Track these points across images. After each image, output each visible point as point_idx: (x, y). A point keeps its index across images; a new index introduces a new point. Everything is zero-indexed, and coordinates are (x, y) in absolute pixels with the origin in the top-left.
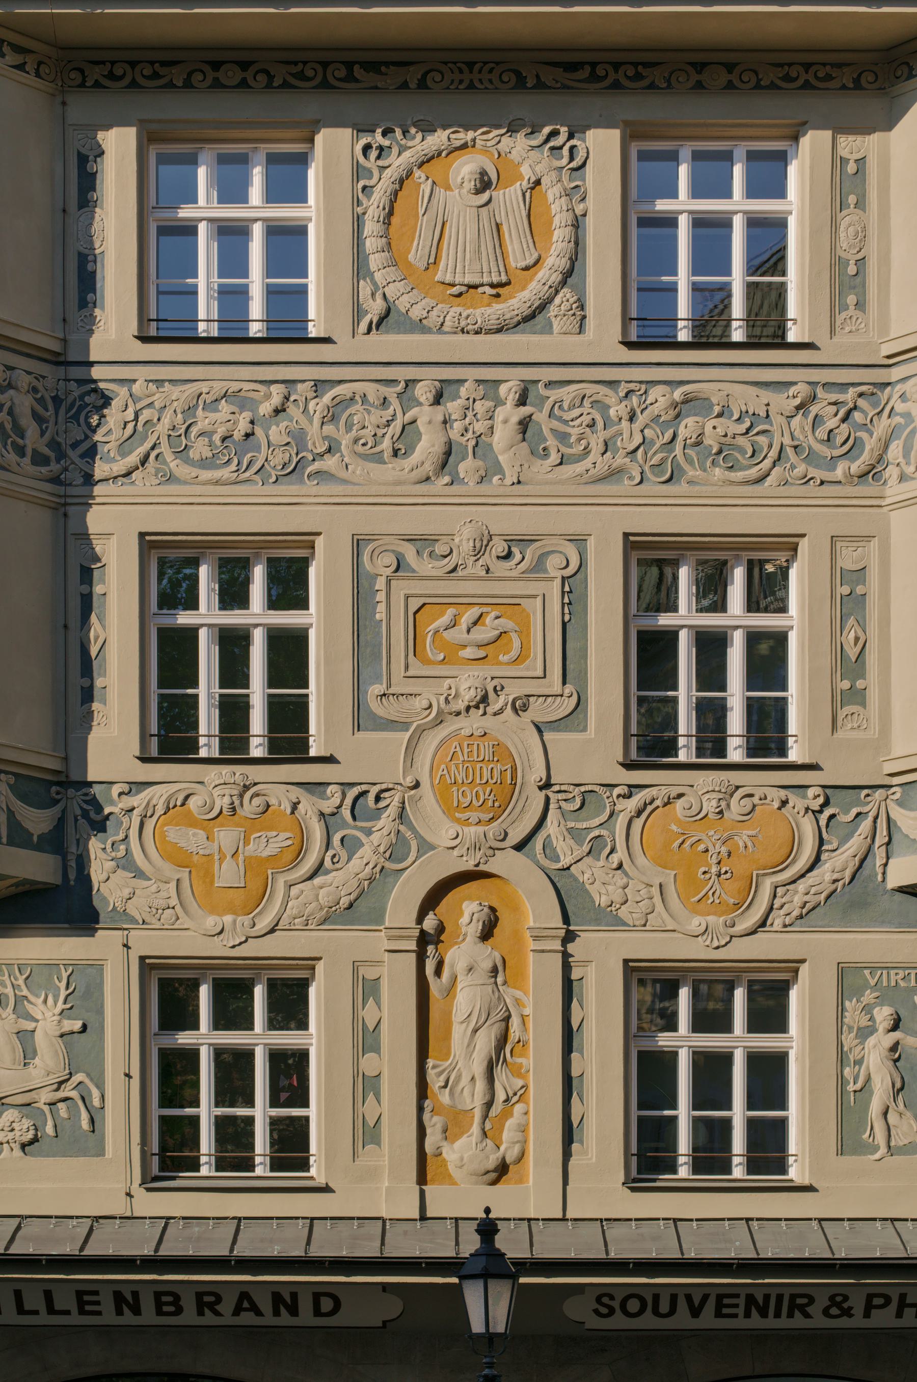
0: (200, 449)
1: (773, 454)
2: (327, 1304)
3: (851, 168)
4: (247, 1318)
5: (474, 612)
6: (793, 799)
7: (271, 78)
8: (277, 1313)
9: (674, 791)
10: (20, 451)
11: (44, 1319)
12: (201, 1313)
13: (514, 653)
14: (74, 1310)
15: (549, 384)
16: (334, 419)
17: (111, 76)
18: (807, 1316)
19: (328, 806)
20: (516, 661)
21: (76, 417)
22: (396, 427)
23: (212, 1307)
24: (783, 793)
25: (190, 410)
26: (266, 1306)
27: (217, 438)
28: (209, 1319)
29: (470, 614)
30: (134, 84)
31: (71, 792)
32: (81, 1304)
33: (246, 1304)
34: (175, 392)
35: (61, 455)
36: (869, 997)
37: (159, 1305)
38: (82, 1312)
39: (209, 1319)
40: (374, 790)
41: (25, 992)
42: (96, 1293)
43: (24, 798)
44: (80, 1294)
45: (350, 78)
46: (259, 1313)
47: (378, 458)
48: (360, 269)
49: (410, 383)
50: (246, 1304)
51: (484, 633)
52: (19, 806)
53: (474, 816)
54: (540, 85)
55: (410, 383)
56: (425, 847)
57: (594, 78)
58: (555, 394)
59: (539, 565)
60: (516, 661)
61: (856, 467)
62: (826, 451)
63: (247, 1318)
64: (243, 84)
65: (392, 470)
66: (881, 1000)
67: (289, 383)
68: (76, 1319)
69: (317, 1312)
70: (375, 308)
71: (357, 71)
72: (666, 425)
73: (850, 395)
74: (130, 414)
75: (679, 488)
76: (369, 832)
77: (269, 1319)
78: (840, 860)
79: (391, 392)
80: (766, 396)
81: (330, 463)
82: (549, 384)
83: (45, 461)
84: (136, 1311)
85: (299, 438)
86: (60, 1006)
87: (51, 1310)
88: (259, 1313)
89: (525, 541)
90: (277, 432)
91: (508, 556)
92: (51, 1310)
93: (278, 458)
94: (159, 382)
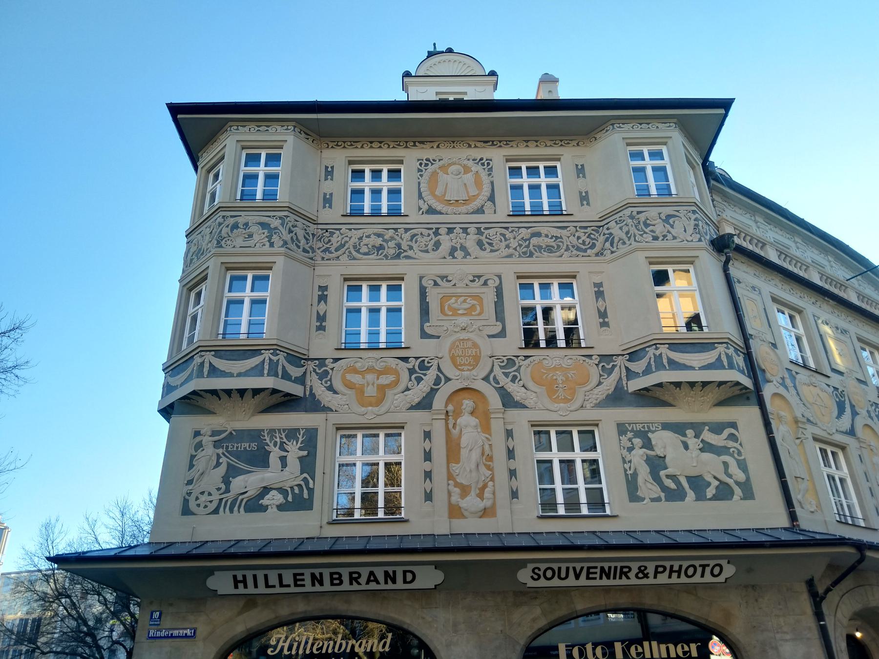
0: (364, 249)
1: (565, 247)
2: (409, 577)
3: (580, 167)
4: (373, 586)
5: (463, 298)
6: (587, 360)
7: (389, 146)
8: (386, 583)
9: (542, 358)
10: (299, 247)
11: (278, 590)
12: (351, 584)
13: (477, 312)
14: (292, 584)
15: (486, 229)
16: (411, 240)
17: (337, 145)
18: (628, 578)
19: (410, 366)
20: (479, 314)
21: (320, 240)
22: (433, 242)
23: (356, 580)
24: (584, 358)
25: (361, 238)
26: (381, 578)
27: (370, 246)
28: (355, 587)
29: (462, 299)
30: (344, 147)
31: (309, 362)
32: (296, 580)
33: (372, 578)
34: (355, 232)
35: (314, 251)
36: (630, 435)
37: (332, 579)
38: (296, 585)
39: (355, 587)
40: (427, 360)
41: (285, 440)
42: (303, 574)
43: (289, 362)
44: (295, 575)
45: (415, 145)
46: (378, 583)
47: (427, 251)
48: (420, 196)
49: (438, 229)
50: (372, 578)
51: (466, 306)
52: (287, 365)
53: (466, 368)
54: (476, 147)
55: (438, 229)
56: (448, 379)
57: (493, 145)
58: (486, 232)
59: (485, 283)
60: (479, 314)
61: (595, 251)
62: (584, 247)
63: (373, 586)
64: (380, 147)
65: (432, 255)
66: (635, 436)
67: (396, 230)
68: (293, 589)
69: (405, 582)
70: (425, 207)
71: (417, 144)
72: (526, 240)
73: (589, 230)
74: (340, 238)
75: (534, 258)
76: (425, 375)
77: (382, 586)
78: (609, 384)
79: (431, 232)
80: (560, 231)
81: (410, 253)
82: (486, 229)
83: (308, 252)
84: (321, 584)
85: (399, 246)
86: (299, 445)
87: (282, 585)
88: (378, 583)
89: (479, 277)
90: (392, 244)
91: (473, 281)
92: (282, 585)
93: (392, 251)
94: (350, 230)
